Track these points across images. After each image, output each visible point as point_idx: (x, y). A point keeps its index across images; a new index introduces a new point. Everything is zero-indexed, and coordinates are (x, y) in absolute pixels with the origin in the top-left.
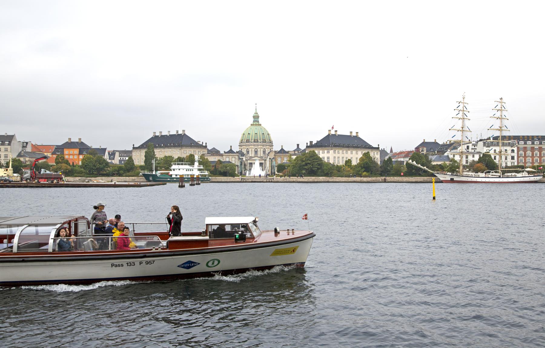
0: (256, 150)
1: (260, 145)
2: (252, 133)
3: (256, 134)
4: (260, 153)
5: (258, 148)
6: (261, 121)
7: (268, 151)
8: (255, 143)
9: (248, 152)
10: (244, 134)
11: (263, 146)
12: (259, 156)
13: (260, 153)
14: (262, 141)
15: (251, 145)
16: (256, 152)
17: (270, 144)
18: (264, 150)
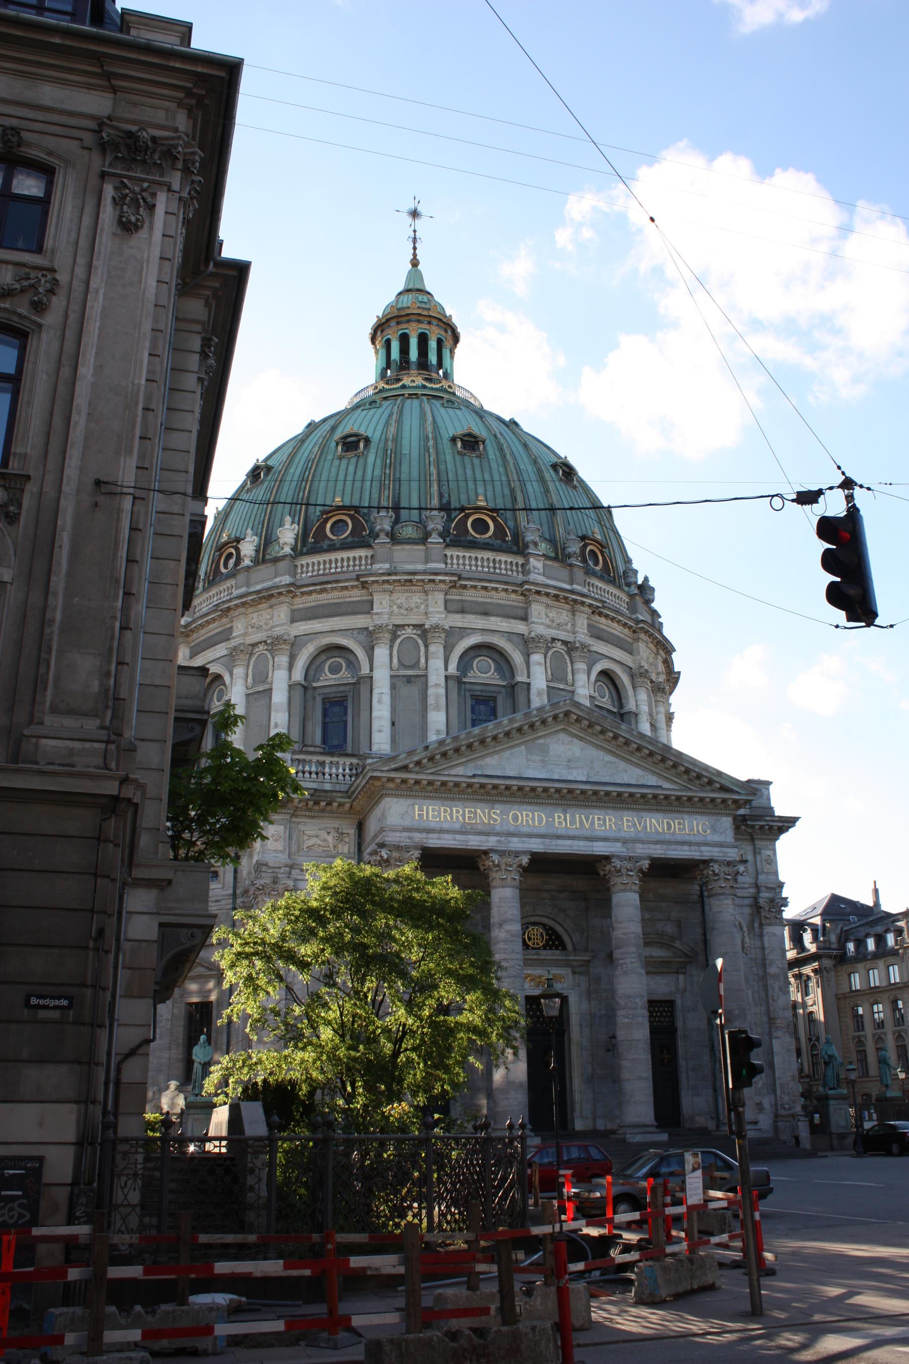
5: (527, 644)
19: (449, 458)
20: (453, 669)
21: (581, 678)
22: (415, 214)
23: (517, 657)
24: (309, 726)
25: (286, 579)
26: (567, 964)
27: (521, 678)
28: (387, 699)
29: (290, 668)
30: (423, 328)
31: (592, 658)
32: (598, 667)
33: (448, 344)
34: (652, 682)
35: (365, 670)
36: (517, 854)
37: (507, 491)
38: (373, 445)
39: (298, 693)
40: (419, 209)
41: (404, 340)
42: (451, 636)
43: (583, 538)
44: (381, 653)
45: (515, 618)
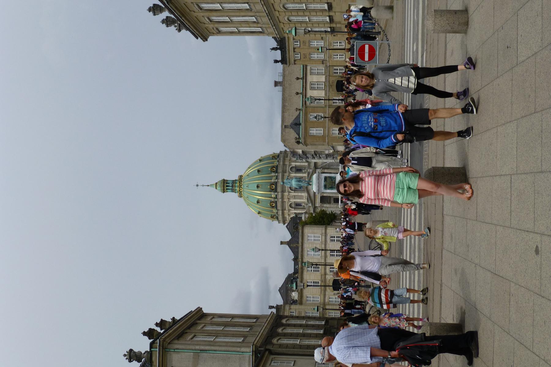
3: (258, 187)
6: (232, 176)
7: (295, 162)
8: (279, 189)
9: (298, 205)
10: (259, 213)
11: (284, 172)
14: (273, 174)
15: (282, 198)
17: (282, 156)
18: (294, 169)
19: (262, 190)
20: (293, 192)
22: (197, 185)
28: (297, 200)
29: (292, 210)
31: (290, 173)
32: (290, 171)
33: (226, 182)
35: (293, 202)
38: (259, 199)
39: (295, 209)
40: (196, 184)
41: (227, 189)
42: (289, 192)
43: (271, 172)
44: (291, 200)
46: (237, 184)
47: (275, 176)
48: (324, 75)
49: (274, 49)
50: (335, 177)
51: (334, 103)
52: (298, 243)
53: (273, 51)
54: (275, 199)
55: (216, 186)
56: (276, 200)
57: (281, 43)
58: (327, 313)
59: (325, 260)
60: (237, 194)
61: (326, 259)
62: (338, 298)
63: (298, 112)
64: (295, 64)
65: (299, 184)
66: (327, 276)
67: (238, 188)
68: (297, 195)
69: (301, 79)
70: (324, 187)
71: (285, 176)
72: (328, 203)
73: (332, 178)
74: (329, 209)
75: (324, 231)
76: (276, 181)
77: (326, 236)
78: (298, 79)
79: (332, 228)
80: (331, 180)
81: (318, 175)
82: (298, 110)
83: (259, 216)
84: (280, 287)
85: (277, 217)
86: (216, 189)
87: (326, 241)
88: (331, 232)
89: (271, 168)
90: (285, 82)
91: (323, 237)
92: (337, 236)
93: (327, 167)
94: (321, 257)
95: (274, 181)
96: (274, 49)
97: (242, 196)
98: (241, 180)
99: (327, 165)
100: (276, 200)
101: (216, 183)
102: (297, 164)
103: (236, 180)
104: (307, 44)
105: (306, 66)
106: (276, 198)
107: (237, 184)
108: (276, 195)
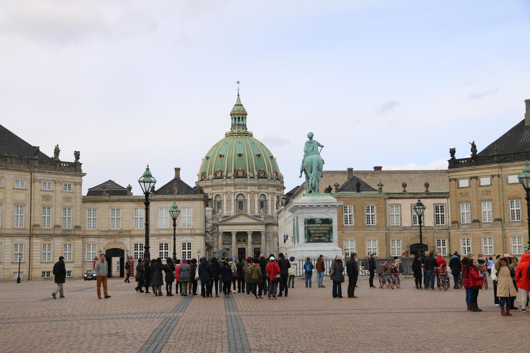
0: (241, 198)
1: (252, 185)
2: (230, 154)
3: (240, 155)
4: (252, 207)
5: (247, 193)
6: (251, 125)
7: (272, 200)
8: (238, 181)
10: (207, 158)
11: (259, 186)
12: (249, 213)
13: (252, 207)
14: (256, 173)
15: (227, 185)
16: (241, 205)
17: (278, 183)
19: (236, 159)
20: (235, 198)
21: (256, 197)
22: (238, 82)
23: (245, 195)
24: (216, 206)
25: (210, 184)
26: (245, 244)
27: (246, 199)
30: (239, 116)
31: (258, 193)
32: (260, 194)
33: (244, 117)
34: (273, 193)
35: (223, 199)
36: (235, 232)
37: (246, 165)
38: (224, 157)
40: (239, 81)
41: (235, 118)
42: (235, 193)
43: (259, 171)
44: (225, 196)
45: (245, 189)
46: (242, 131)
47: (254, 175)
48: (435, 225)
49: (474, 146)
50: (331, 242)
51: (392, 241)
52: (178, 194)
53: (471, 146)
54: (225, 176)
55: (238, 105)
56: (225, 178)
57: (485, 157)
58: (69, 242)
59: (153, 236)
60: (230, 131)
61: (155, 236)
62: (94, 258)
63: (377, 188)
64: (450, 180)
65: (312, 168)
66: (129, 238)
67: (237, 132)
68: (231, 203)
69: (427, 191)
70: (309, 218)
71: (253, 188)
72: (223, 241)
73: (330, 235)
74: (215, 243)
75: (198, 232)
76: (248, 177)
77: (191, 235)
78: (427, 185)
79: (202, 245)
80: (324, 234)
81: (334, 206)
82: (380, 187)
83: (204, 156)
84: (115, 182)
85: (203, 180)
86: (235, 105)
87: (183, 236)
88: (197, 243)
89: (263, 171)
90: (399, 175)
91: (189, 232)
92: (190, 252)
93: (268, 239)
94: (159, 230)
95: (248, 175)
96: (474, 146)
97: (227, 136)
98: (247, 135)
99: (270, 239)
100: (225, 178)
101: (242, 105)
102: (270, 202)
103: (246, 129)
104: (484, 197)
105: (447, 198)
106: (227, 178)
107: (241, 130)
108: (231, 178)
